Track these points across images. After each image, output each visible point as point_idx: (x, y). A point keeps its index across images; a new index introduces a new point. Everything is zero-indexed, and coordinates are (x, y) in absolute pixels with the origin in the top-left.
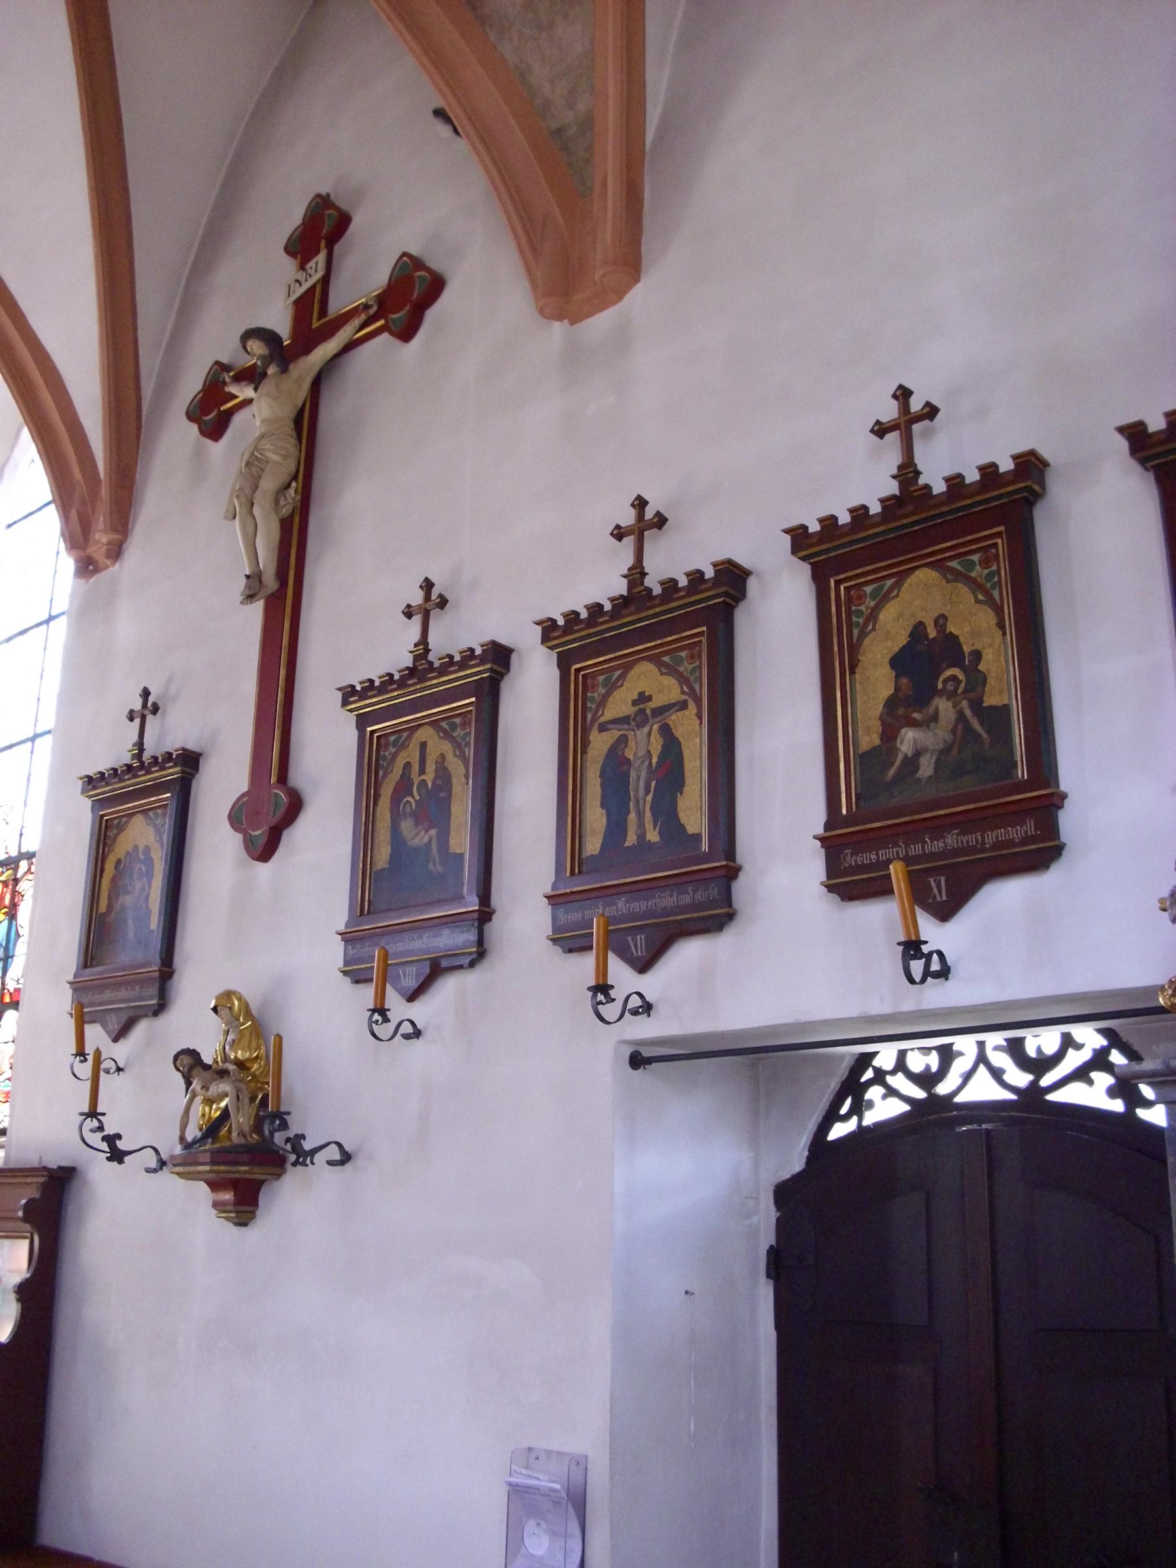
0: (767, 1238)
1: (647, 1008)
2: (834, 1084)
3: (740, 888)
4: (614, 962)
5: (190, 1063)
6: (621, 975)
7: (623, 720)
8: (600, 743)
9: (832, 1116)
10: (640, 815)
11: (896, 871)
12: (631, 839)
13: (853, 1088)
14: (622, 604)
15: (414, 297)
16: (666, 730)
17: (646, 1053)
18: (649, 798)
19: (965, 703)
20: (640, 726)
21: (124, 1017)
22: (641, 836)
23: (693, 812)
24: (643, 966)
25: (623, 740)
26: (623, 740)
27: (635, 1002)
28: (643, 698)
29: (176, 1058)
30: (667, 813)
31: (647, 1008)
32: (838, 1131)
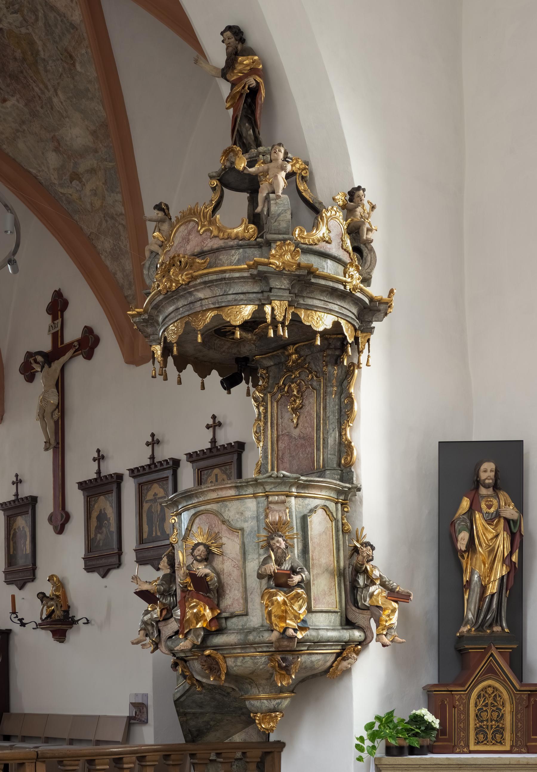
5: (42, 596)
21: (22, 582)
29: (38, 595)
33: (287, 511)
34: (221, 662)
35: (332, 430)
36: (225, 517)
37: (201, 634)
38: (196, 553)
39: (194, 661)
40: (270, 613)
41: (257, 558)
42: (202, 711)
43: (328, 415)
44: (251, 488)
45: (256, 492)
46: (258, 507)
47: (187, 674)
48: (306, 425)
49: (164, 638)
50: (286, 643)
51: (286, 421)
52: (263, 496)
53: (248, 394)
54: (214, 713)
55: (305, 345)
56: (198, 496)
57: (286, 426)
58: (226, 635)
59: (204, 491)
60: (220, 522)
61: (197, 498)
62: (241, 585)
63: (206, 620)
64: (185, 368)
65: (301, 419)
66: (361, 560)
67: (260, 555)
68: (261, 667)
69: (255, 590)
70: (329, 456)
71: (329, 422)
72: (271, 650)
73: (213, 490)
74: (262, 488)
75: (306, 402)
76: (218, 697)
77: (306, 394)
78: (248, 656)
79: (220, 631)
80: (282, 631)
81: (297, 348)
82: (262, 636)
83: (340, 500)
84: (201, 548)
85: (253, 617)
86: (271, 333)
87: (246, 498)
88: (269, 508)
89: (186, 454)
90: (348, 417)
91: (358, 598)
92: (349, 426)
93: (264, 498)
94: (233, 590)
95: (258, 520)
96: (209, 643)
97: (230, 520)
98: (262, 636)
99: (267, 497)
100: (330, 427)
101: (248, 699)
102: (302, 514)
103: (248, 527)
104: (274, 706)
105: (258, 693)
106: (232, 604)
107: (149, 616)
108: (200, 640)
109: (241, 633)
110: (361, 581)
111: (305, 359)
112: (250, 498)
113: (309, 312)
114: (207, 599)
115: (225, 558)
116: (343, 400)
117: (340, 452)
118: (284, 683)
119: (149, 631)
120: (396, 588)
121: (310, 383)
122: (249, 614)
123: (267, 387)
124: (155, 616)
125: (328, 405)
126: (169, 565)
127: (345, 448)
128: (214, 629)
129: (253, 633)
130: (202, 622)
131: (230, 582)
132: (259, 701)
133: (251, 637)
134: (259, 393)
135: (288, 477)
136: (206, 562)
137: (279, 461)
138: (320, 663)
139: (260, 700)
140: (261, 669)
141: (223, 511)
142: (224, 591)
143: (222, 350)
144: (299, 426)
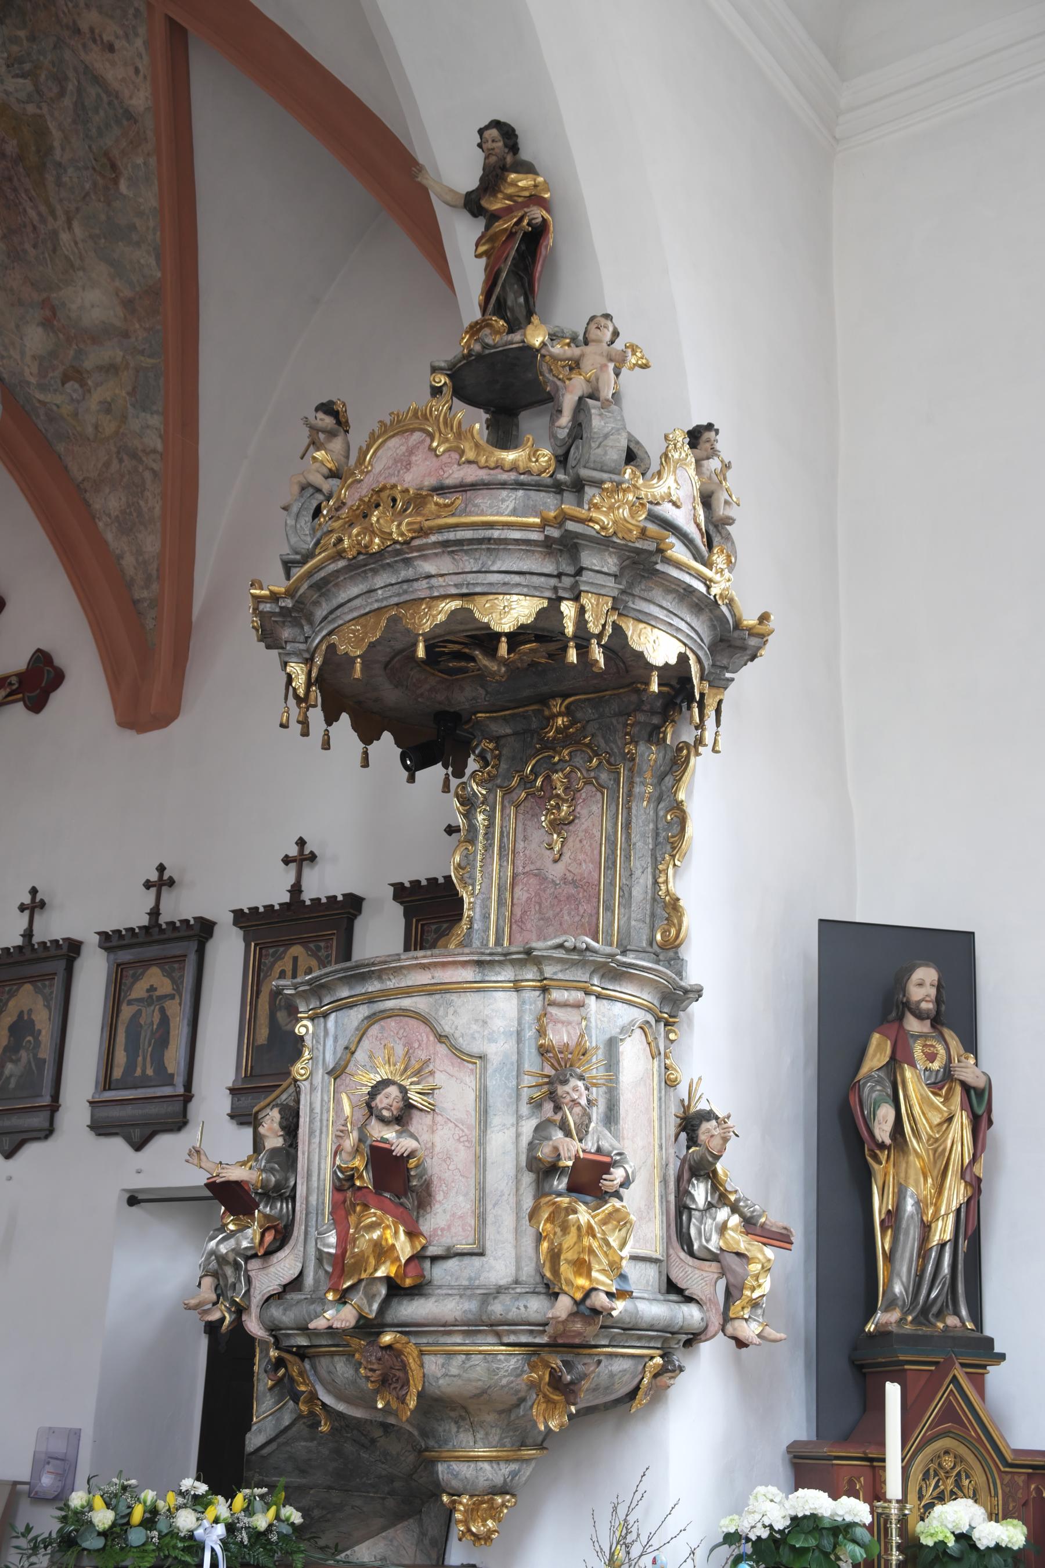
3: (192, 1106)
7: (139, 1000)
8: (127, 1012)
10: (144, 1059)
12: (138, 1072)
15: (43, 685)
16: (162, 1011)
18: (150, 1049)
20: (149, 1005)
22: (144, 1071)
23: (174, 1058)
26: (138, 1013)
33: (584, 1023)
34: (412, 1363)
35: (640, 871)
36: (447, 1028)
37: (380, 1293)
38: (381, 1101)
39: (336, 1358)
40: (555, 1256)
41: (513, 1125)
42: (304, 1481)
43: (634, 840)
45: (520, 978)
46: (521, 1012)
47: (303, 1388)
48: (581, 857)
49: (258, 1297)
50: (578, 1326)
51: (534, 846)
52: (534, 988)
53: (446, 788)
54: (329, 1488)
55: (588, 699)
56: (384, 977)
57: (534, 856)
58: (433, 1299)
59: (402, 967)
60: (432, 1038)
61: (380, 978)
62: (472, 1182)
63: (398, 1259)
64: (337, 720)
66: (719, 1147)
67: (519, 1117)
68: (504, 1382)
69: (505, 1198)
70: (633, 923)
71: (635, 854)
72: (538, 1340)
73: (424, 967)
74: (535, 969)
75: (582, 810)
76: (349, 1448)
77: (584, 796)
78: (480, 1353)
79: (419, 1290)
80: (579, 1296)
81: (570, 704)
82: (526, 1307)
83: (666, 1016)
84: (393, 1090)
85: (495, 1259)
86: (572, 656)
89: (233, 911)
90: (674, 848)
91: (693, 1232)
92: (675, 865)
93: (537, 993)
94: (452, 1194)
95: (519, 1040)
96: (390, 1317)
97: (457, 1035)
98: (526, 1307)
99: (545, 990)
100: (636, 864)
101: (444, 1460)
102: (608, 1036)
103: (496, 1054)
104: (505, 1480)
105: (472, 1444)
106: (449, 1227)
107: (232, 1243)
108: (375, 1306)
109: (470, 1297)
110: (700, 1192)
111: (584, 727)
112: (504, 989)
113: (642, 626)
114: (401, 1209)
115: (439, 1118)
116: (661, 813)
117: (653, 915)
118: (553, 1425)
120: (760, 1216)
121: (592, 774)
122: (488, 1252)
123: (495, 776)
124: (245, 1244)
125: (634, 820)
126: (283, 1128)
127: (669, 910)
128: (408, 1282)
129: (502, 1297)
130: (388, 1263)
131: (446, 1175)
132: (473, 1465)
133: (497, 1308)
134: (477, 784)
135: (595, 952)
136: (398, 1124)
137: (514, 927)
138: (625, 1379)
139: (472, 1461)
140: (503, 1387)
141: (441, 1012)
142: (430, 1195)
143: (419, 692)
144: (563, 857)
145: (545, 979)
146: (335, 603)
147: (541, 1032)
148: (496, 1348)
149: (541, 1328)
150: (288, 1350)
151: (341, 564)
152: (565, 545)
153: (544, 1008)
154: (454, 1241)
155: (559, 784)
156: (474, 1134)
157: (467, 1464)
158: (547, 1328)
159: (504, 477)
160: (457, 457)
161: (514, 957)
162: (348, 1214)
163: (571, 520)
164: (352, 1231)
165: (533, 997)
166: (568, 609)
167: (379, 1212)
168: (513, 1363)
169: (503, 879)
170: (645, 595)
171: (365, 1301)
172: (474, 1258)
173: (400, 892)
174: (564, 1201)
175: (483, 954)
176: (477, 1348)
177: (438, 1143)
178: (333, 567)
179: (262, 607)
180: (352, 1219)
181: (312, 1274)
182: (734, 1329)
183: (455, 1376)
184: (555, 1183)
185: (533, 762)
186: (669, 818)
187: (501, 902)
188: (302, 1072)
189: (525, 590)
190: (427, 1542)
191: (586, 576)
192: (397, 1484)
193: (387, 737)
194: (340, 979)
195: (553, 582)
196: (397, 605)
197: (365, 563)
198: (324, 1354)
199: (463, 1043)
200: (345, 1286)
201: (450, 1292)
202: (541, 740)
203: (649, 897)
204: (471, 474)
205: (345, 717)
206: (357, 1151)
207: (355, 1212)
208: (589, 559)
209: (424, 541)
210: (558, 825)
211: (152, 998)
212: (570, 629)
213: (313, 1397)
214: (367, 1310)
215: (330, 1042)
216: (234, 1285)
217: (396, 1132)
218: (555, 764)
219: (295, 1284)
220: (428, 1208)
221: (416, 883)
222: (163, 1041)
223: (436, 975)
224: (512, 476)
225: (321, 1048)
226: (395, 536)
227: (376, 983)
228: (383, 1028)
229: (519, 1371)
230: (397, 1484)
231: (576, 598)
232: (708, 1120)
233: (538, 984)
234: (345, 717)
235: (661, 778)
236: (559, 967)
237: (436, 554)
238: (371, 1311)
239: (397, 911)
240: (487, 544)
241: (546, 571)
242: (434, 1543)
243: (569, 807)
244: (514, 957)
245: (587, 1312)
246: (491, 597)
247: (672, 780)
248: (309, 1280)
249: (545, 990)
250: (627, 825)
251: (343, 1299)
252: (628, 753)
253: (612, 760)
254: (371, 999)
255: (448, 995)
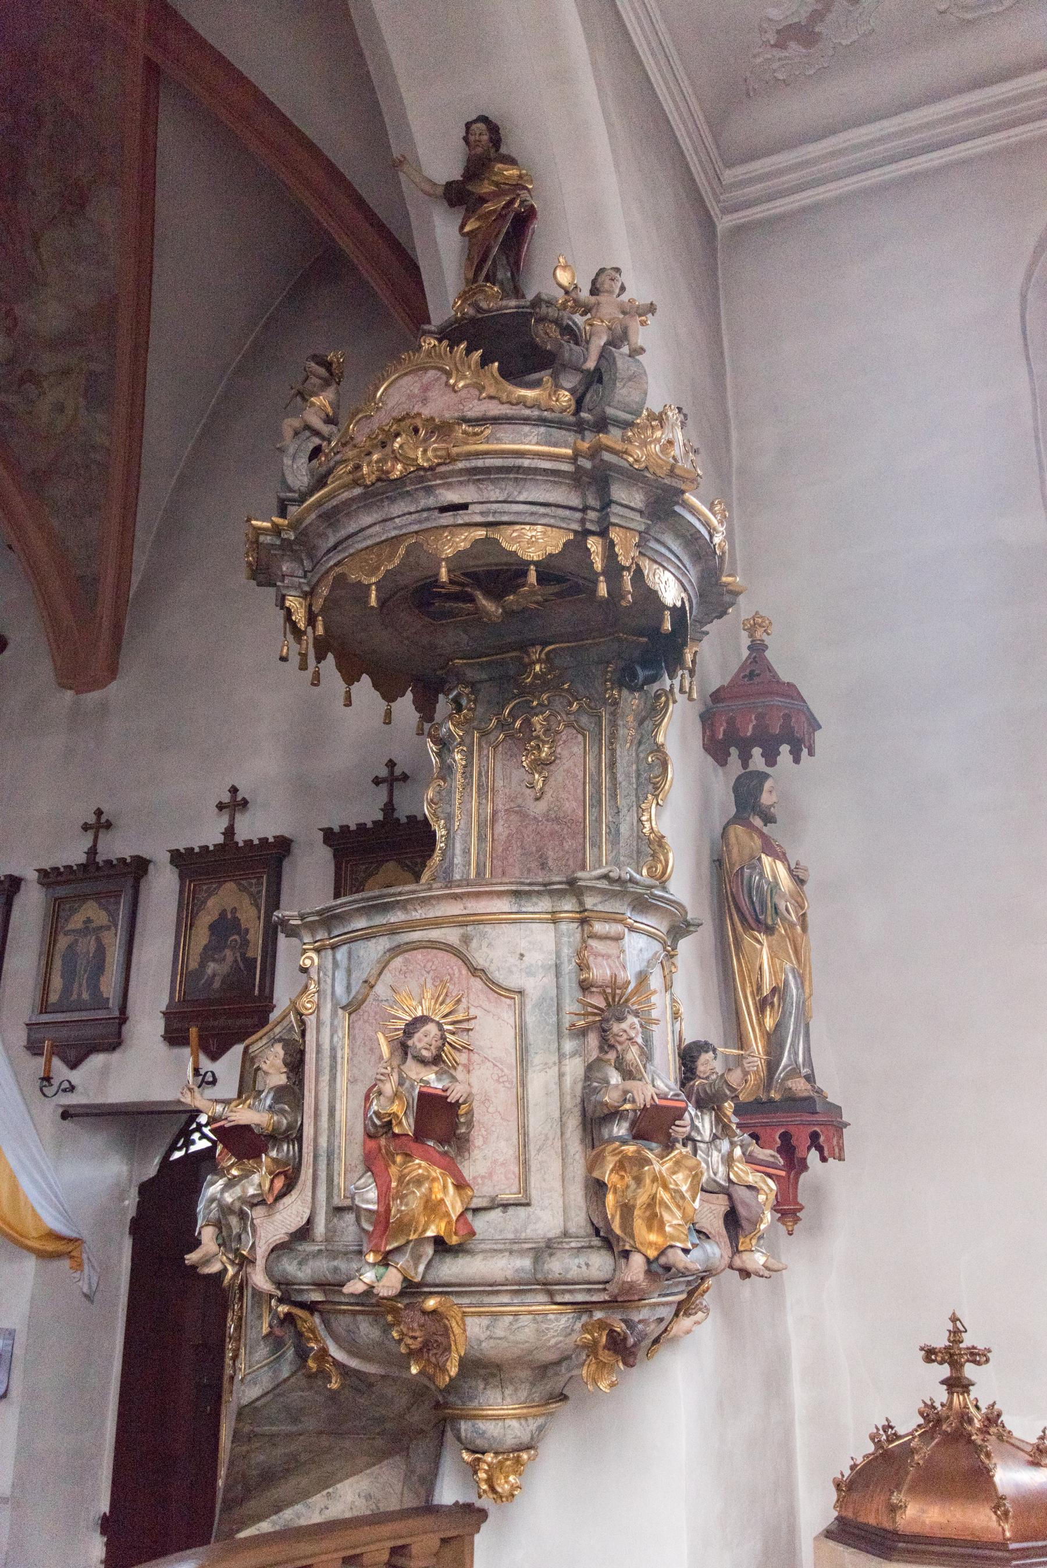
0: (132, 1213)
1: (72, 1088)
2: (176, 1130)
3: (125, 1028)
4: (56, 1062)
6: (60, 1069)
8: (63, 942)
9: (173, 1148)
10: (80, 986)
11: (193, 1031)
12: (75, 997)
13: (185, 1135)
14: (83, 867)
16: (98, 940)
17: (72, 1111)
19: (238, 954)
20: (86, 936)
23: (110, 985)
24: (73, 1066)
25: (76, 941)
27: (66, 1085)
28: (89, 921)
30: (95, 987)
31: (72, 1088)
32: (177, 1155)
39: (360, 1318)
41: (555, 1064)
42: (294, 1429)
44: (547, 897)
45: (559, 909)
46: (557, 944)
48: (564, 795)
49: (264, 1248)
52: (572, 920)
53: (420, 732)
58: (480, 1257)
60: (464, 971)
65: (552, 782)
67: (561, 1056)
68: (553, 1342)
69: (549, 1142)
72: (595, 1299)
74: (574, 901)
77: (564, 737)
78: (530, 1313)
82: (587, 1265)
84: (431, 1028)
85: (542, 1209)
87: (533, 921)
88: (589, 948)
89: (169, 851)
90: (656, 789)
92: (658, 804)
93: (576, 925)
95: (558, 975)
97: (493, 968)
98: (587, 1265)
100: (621, 802)
105: (500, 1400)
106: (491, 1175)
107: (237, 1191)
108: (421, 1268)
109: (522, 1253)
112: (541, 921)
113: (655, 566)
115: (475, 1057)
116: (642, 755)
117: (639, 852)
119: (230, 1228)
121: (572, 718)
123: (471, 720)
124: (251, 1191)
126: (286, 1064)
130: (437, 1221)
132: (500, 1423)
133: (557, 1266)
135: (637, 883)
137: (495, 862)
140: (550, 1347)
145: (586, 910)
146: (343, 533)
147: (582, 966)
148: (548, 1307)
149: (601, 1286)
150: (302, 1305)
151: (358, 491)
152: (595, 479)
153: (584, 942)
154: (498, 1192)
155: (538, 727)
156: (512, 1074)
157: (494, 1423)
158: (607, 1286)
159: (527, 412)
160: (477, 393)
161: (555, 887)
162: (387, 1166)
163: (606, 450)
164: (394, 1184)
165: (570, 929)
166: (594, 544)
167: (423, 1163)
168: (564, 1321)
169: (483, 817)
170: (659, 536)
171: (411, 1263)
172: (519, 1208)
173: (329, 836)
174: (630, 1149)
175: (523, 883)
176: (527, 1308)
177: (481, 1084)
178: (346, 495)
179: (262, 539)
180: (394, 1170)
181: (323, 1221)
182: (743, 1262)
183: (500, 1339)
184: (615, 1129)
185: (511, 706)
186: (650, 759)
187: (481, 838)
188: (309, 1005)
189: (552, 521)
190: (415, 1478)
191: (615, 509)
192: (388, 1426)
193: (366, 679)
194: (358, 909)
195: (578, 515)
196: (416, 532)
197: (385, 489)
198: (345, 1312)
199: (499, 977)
200: (389, 1248)
201: (495, 1247)
202: (518, 686)
203: (635, 835)
204: (494, 409)
205: (330, 657)
206: (396, 1095)
207: (394, 1162)
208: (619, 493)
209: (451, 467)
210: (541, 765)
211: (88, 928)
212: (598, 566)
213: (324, 1352)
214: (412, 1274)
215: (341, 975)
216: (239, 1237)
217: (436, 1073)
218: (533, 708)
219: (304, 1233)
220: (466, 1154)
221: (345, 829)
222: (99, 966)
223: (469, 905)
224: (536, 413)
225: (329, 981)
226: (420, 461)
227: (399, 913)
228: (407, 960)
229: (569, 1330)
230: (388, 1426)
231: (603, 533)
232: (707, 1052)
233: (578, 916)
234: (330, 657)
235: (641, 723)
236: (599, 899)
237: (461, 483)
238: (416, 1273)
239: (324, 855)
240: (514, 472)
241: (571, 504)
242: (422, 1480)
243: (550, 748)
244: (555, 887)
245: (660, 1271)
246: (518, 527)
247: (651, 723)
248: (320, 1228)
249: (584, 922)
250: (612, 765)
251: (385, 1261)
252: (609, 698)
253: (592, 705)
254: (393, 930)
255: (481, 926)
